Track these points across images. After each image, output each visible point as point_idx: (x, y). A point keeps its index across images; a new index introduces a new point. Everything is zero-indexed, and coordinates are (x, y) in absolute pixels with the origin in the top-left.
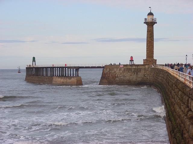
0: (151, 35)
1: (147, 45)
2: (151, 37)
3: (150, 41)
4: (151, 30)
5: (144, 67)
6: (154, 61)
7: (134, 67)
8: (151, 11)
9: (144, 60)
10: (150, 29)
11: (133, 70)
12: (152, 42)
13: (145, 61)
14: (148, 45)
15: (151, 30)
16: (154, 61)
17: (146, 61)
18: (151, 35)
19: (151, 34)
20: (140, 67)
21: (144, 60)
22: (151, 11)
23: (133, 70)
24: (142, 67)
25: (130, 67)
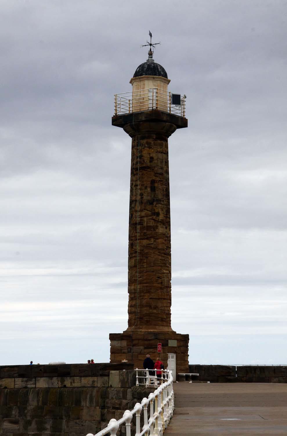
0: (153, 189)
1: (131, 246)
2: (151, 203)
3: (148, 228)
4: (152, 159)
5: (99, 382)
6: (172, 343)
7: (42, 383)
8: (151, 54)
9: (113, 337)
10: (145, 153)
11: (33, 403)
12: (161, 230)
13: (117, 344)
14: (138, 248)
16: (172, 343)
17: (124, 343)
19: (153, 182)
20: (78, 382)
21: (113, 337)
22: (151, 54)
23: (33, 403)
24: (86, 381)
25: (19, 383)
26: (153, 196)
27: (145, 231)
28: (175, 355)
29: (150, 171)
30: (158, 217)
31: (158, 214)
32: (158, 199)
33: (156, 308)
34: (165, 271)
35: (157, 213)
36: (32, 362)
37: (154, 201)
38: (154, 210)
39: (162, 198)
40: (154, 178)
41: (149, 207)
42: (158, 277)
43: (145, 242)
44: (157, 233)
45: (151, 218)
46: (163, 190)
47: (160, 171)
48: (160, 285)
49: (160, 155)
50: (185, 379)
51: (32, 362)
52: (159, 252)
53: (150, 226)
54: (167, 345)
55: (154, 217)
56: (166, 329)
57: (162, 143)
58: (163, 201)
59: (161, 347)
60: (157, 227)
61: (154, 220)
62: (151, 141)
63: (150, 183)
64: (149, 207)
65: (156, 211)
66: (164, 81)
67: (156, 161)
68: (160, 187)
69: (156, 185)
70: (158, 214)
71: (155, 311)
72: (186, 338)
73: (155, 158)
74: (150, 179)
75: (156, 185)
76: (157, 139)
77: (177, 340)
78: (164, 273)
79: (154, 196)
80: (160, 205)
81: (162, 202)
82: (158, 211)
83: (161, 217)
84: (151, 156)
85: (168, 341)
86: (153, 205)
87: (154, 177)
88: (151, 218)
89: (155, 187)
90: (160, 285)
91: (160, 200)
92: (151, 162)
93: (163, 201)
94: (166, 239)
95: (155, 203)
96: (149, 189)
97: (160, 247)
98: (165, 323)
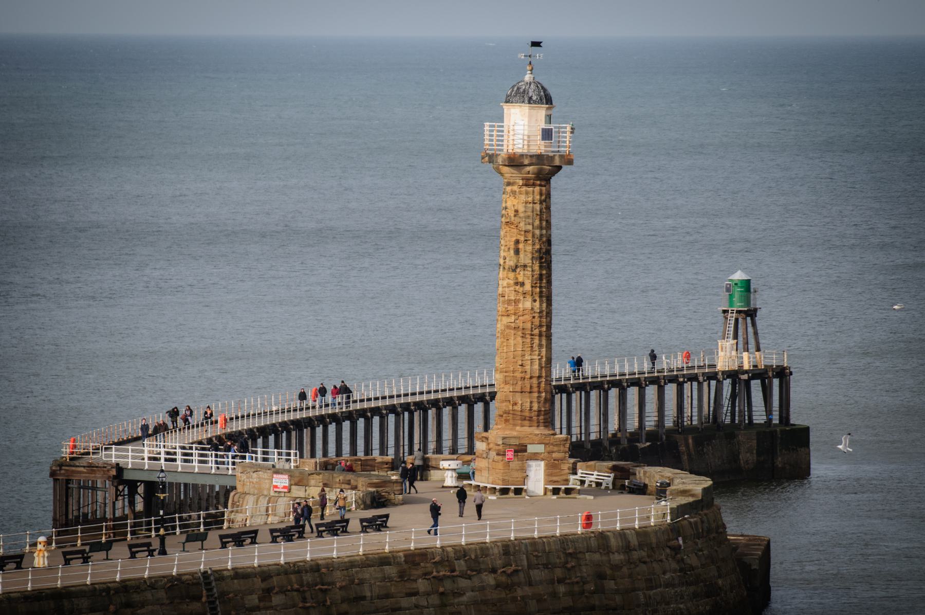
0: (517, 252)
2: (514, 270)
3: (509, 302)
19: (517, 242)
26: (515, 261)
27: (506, 306)
31: (523, 284)
37: (517, 267)
38: (517, 278)
41: (511, 275)
43: (505, 320)
54: (525, 451)
62: (515, 188)
63: (512, 243)
65: (521, 279)
70: (523, 284)
74: (514, 239)
77: (546, 444)
84: (516, 208)
85: (526, 446)
89: (519, 249)
92: (515, 216)
95: (518, 270)
96: (512, 252)
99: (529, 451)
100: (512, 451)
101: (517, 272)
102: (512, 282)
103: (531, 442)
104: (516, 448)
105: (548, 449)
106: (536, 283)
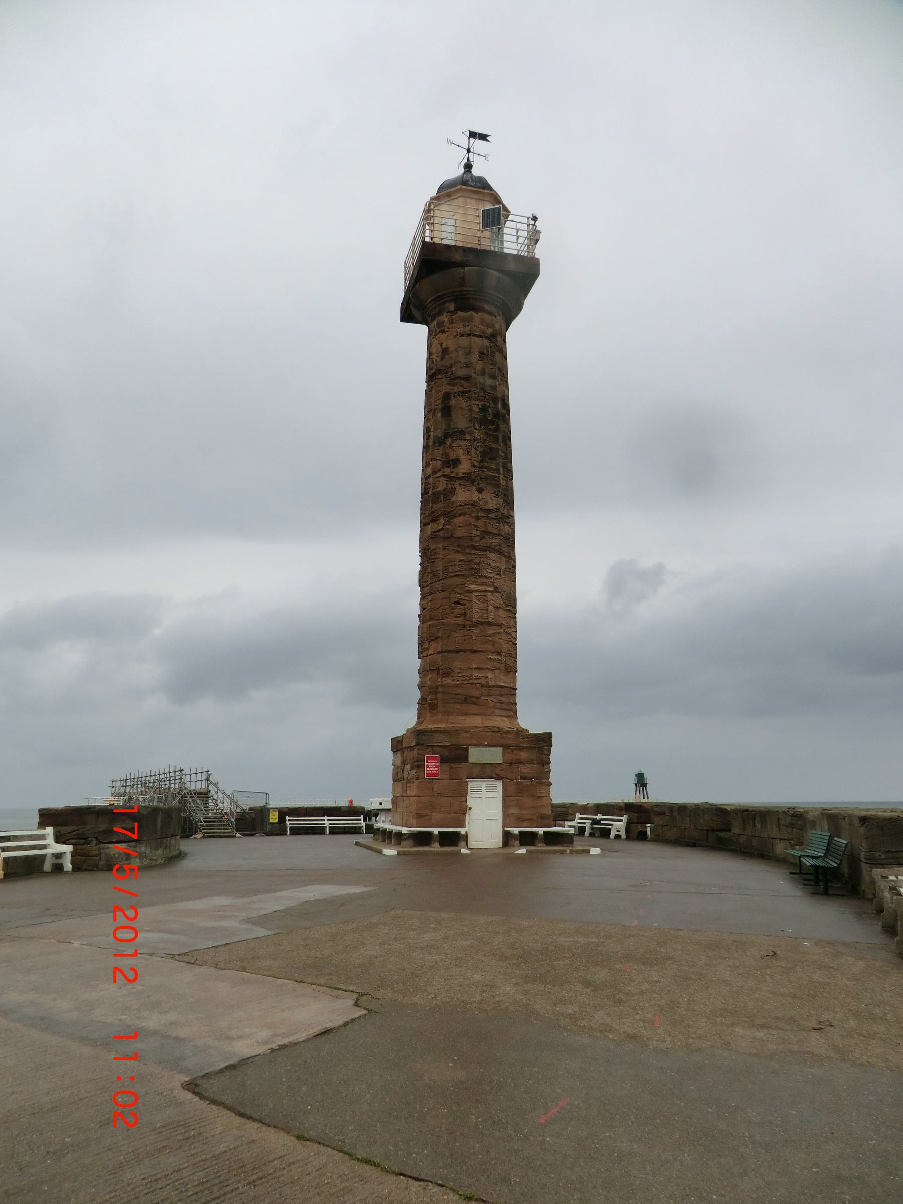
0: (447, 411)
4: (445, 351)
8: (468, 166)
15: (445, 351)
18: (447, 411)
19: (447, 396)
22: (468, 166)
28: (499, 785)
29: (442, 377)
30: (455, 470)
31: (456, 462)
32: (456, 430)
33: (448, 673)
34: (473, 587)
35: (453, 460)
36: (351, 802)
37: (447, 435)
38: (448, 454)
39: (468, 428)
40: (448, 388)
41: (439, 453)
42: (455, 603)
44: (453, 503)
45: (440, 474)
46: (470, 410)
47: (462, 372)
48: (460, 620)
49: (464, 341)
50: (517, 843)
51: (351, 802)
52: (458, 546)
53: (440, 492)
54: (465, 758)
55: (447, 471)
56: (504, 724)
57: (471, 316)
58: (470, 433)
59: (437, 766)
60: (452, 491)
61: (445, 476)
62: (445, 318)
64: (439, 451)
65: (453, 456)
66: (475, 196)
67: (453, 355)
68: (464, 405)
69: (453, 402)
71: (449, 681)
72: (544, 742)
73: (452, 348)
75: (453, 402)
76: (458, 308)
77: (506, 748)
78: (471, 592)
79: (449, 426)
80: (462, 443)
81: (468, 437)
82: (455, 455)
83: (464, 467)
85: (466, 750)
86: (446, 444)
87: (450, 387)
88: (440, 474)
90: (460, 620)
91: (462, 433)
92: (443, 358)
93: (470, 433)
94: (481, 514)
97: (459, 533)
98: (473, 707)
99: (471, 760)
100: (436, 758)
101: (448, 444)
102: (439, 464)
103: (474, 742)
104: (446, 753)
105: (510, 756)
106: (481, 461)
